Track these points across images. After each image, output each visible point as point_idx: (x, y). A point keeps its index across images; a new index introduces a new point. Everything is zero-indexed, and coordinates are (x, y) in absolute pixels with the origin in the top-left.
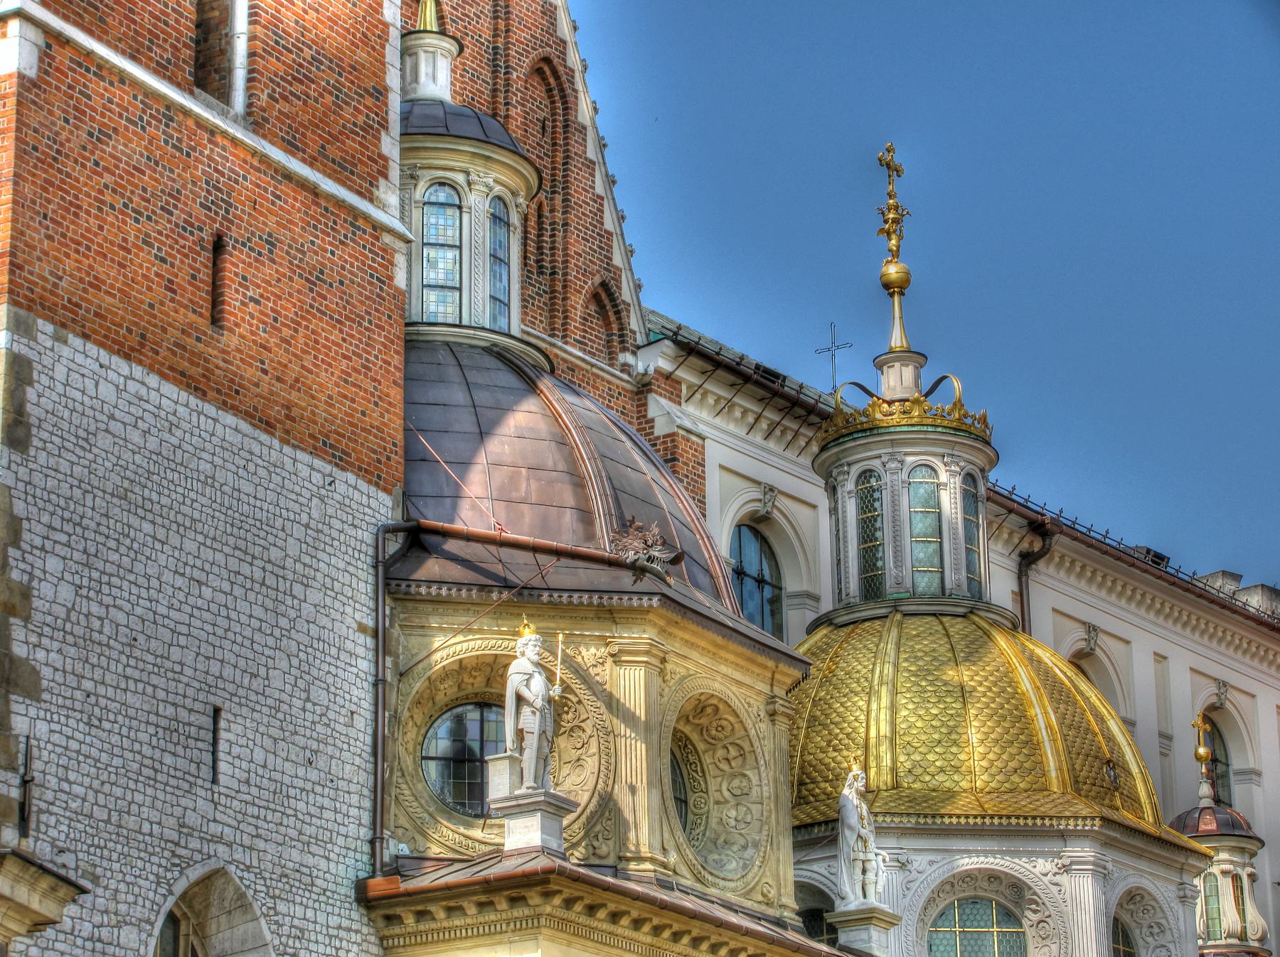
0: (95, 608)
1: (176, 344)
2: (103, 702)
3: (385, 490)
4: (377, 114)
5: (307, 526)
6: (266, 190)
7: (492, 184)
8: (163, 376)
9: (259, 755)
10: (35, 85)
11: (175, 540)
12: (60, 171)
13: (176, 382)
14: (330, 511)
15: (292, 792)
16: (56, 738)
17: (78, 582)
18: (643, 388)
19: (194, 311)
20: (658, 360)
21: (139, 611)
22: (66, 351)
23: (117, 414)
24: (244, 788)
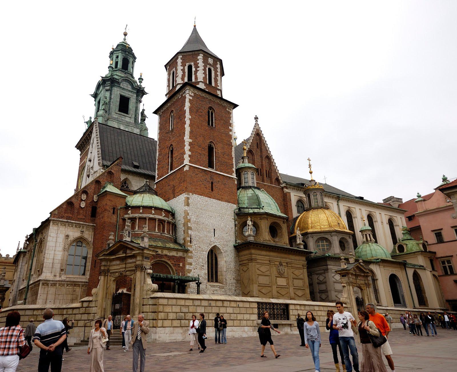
0: (198, 220)
11: (208, 213)
18: (282, 188)
20: (284, 185)
22: (193, 196)
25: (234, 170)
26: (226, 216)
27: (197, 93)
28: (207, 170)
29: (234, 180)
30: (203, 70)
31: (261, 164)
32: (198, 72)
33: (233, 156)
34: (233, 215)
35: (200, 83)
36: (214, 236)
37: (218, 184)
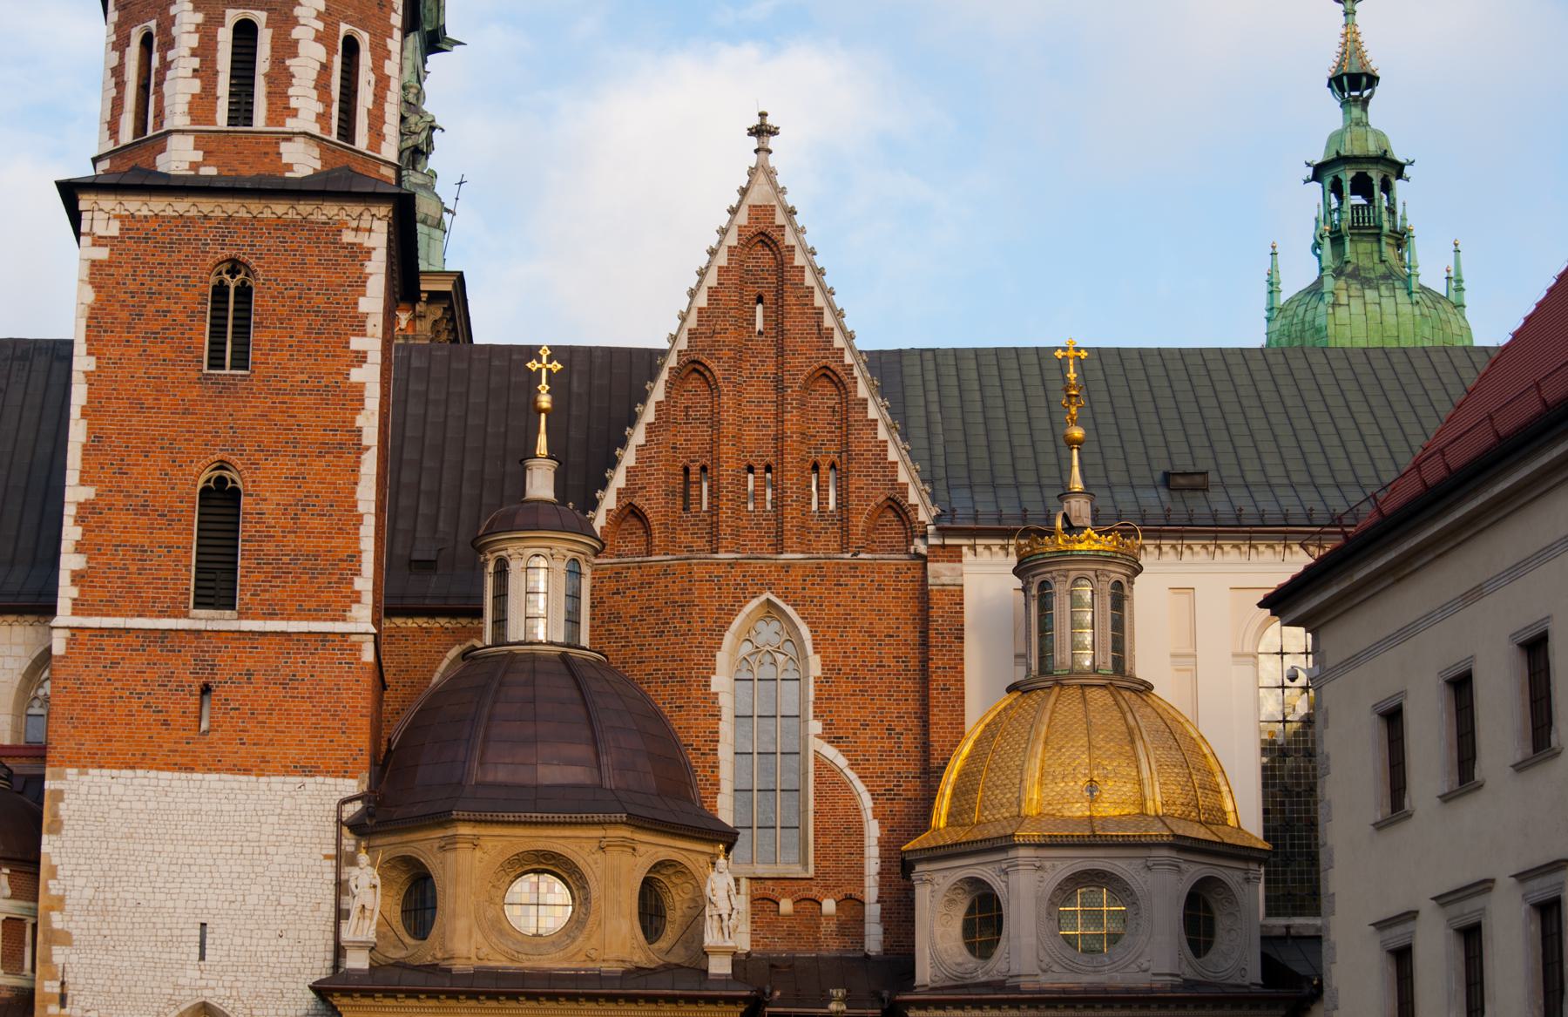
0: (109, 895)
1: (169, 751)
2: (115, 938)
3: (351, 777)
4: (351, 570)
5: (279, 815)
6: (244, 648)
7: (521, 551)
8: (159, 769)
9: (238, 941)
10: (63, 657)
11: (170, 848)
12: (82, 693)
13: (169, 770)
14: (299, 802)
15: (264, 954)
16: (84, 961)
17: (96, 885)
19: (185, 730)
20: (932, 541)
21: (140, 889)
23: (124, 798)
24: (226, 959)
25: (364, 584)
26: (282, 851)
27: (145, 212)
28: (177, 630)
29: (354, 644)
30: (194, 53)
31: (771, 431)
32: (169, 74)
33: (361, 508)
34: (331, 828)
35: (174, 142)
36: (202, 957)
37: (247, 689)
